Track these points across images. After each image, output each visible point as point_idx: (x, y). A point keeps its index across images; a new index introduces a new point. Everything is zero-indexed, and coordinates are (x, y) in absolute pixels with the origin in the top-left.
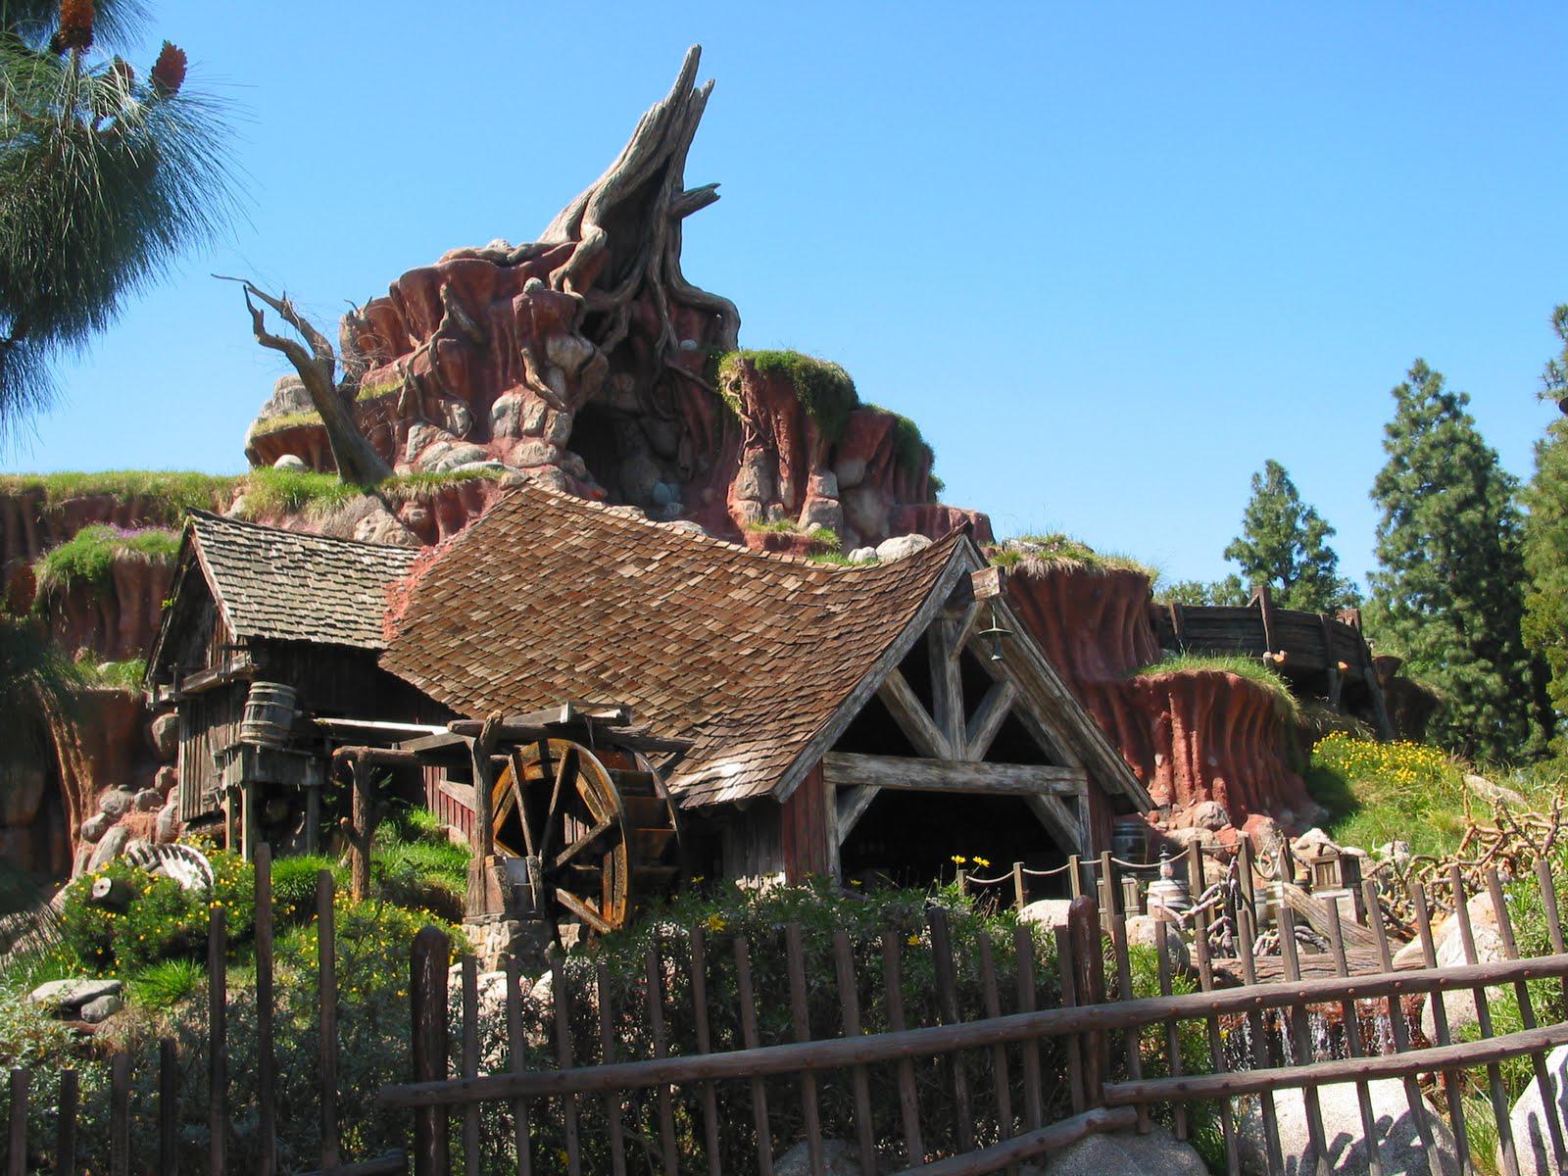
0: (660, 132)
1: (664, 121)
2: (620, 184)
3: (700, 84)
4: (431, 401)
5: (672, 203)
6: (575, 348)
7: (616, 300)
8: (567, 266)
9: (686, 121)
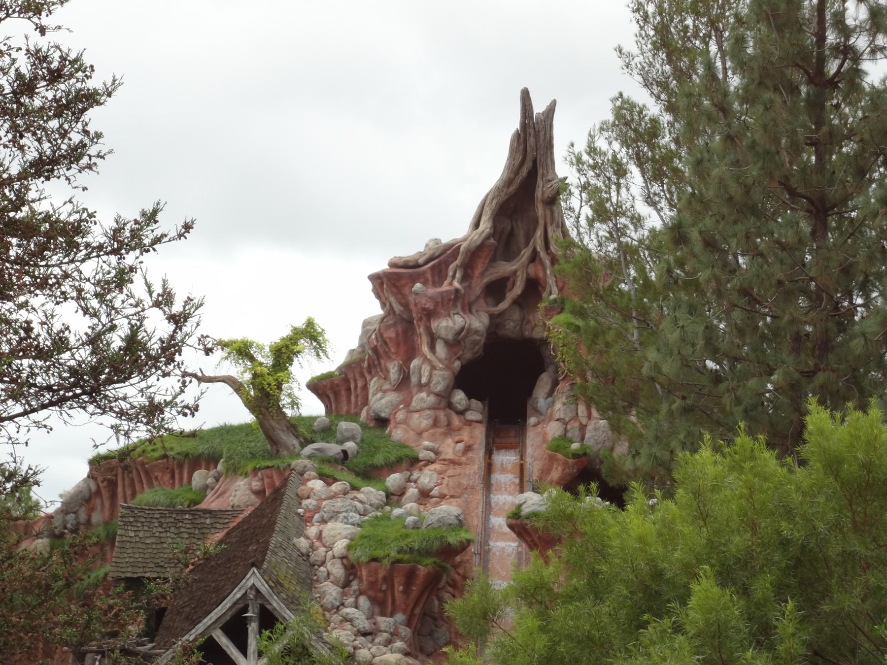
0: (522, 147)
1: (522, 140)
2: (504, 187)
3: (539, 108)
4: (382, 362)
5: (543, 192)
6: (447, 327)
7: (514, 268)
8: (458, 262)
9: (537, 136)
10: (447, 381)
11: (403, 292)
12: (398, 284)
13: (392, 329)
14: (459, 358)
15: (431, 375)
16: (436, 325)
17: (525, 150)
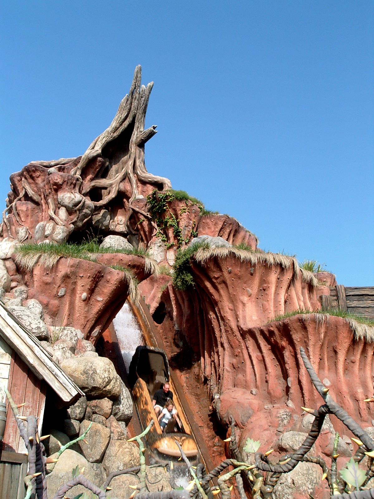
1: (129, 102)
4: (13, 228)
5: (137, 138)
10: (66, 234)
11: (37, 181)
12: (34, 175)
13: (24, 206)
14: (73, 223)
15: (54, 229)
16: (62, 195)
17: (130, 109)
